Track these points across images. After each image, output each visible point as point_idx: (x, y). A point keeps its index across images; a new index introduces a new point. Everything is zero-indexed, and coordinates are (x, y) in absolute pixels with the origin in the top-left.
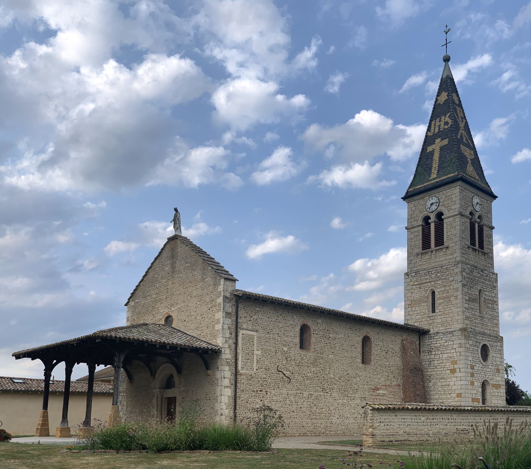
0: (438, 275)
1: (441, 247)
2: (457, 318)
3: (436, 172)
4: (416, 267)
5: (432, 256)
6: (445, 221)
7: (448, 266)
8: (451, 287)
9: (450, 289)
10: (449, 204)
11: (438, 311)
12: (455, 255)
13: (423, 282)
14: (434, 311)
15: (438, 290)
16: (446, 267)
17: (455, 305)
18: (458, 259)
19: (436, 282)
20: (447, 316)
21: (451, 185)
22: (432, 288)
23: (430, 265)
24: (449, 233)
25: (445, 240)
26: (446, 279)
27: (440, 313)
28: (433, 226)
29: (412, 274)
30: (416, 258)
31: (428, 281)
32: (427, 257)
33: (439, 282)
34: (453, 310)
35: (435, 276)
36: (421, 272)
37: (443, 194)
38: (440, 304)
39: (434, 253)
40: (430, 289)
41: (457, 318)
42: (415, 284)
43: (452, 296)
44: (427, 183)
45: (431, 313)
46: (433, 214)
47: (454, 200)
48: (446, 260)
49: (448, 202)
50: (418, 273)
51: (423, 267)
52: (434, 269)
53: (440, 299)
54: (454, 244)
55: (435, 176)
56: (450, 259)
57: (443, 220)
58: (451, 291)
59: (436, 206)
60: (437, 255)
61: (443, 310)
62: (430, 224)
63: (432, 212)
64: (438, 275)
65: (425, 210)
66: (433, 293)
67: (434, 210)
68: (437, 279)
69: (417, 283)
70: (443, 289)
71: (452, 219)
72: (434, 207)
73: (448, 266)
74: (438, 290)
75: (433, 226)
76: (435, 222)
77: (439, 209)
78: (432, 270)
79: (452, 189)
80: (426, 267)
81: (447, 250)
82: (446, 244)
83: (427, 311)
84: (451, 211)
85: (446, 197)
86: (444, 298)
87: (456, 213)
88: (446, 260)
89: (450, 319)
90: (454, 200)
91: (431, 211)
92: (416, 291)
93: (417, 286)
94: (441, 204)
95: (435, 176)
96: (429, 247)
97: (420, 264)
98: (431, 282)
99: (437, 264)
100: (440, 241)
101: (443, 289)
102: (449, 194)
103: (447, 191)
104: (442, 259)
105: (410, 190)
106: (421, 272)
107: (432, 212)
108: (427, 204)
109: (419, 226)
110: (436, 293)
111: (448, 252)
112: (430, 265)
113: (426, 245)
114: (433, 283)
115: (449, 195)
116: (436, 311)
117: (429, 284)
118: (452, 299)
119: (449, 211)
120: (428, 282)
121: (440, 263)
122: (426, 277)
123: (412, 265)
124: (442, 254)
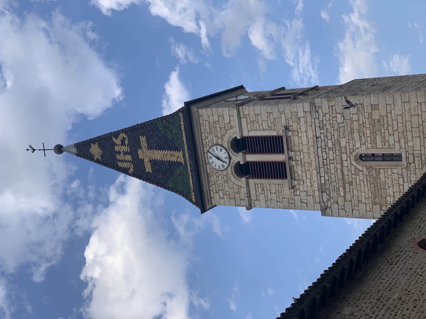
0: (330, 145)
1: (284, 140)
2: (413, 103)
3: (176, 153)
4: (314, 192)
5: (298, 158)
6: (245, 134)
7: (317, 125)
8: (355, 117)
9: (358, 120)
10: (222, 126)
11: (397, 145)
12: (301, 114)
13: (340, 176)
14: (397, 158)
15: (358, 145)
16: (317, 129)
17: (389, 109)
18: (307, 107)
19: (343, 150)
20: (409, 127)
21: (195, 122)
22: (352, 158)
23: (313, 163)
24: (265, 127)
25: (274, 134)
26: (338, 130)
27: (402, 141)
28: (252, 158)
29: (325, 200)
30: (298, 192)
31: (339, 166)
32: (298, 170)
33: (343, 144)
34: (397, 113)
35: (331, 153)
36: (323, 182)
37: (207, 137)
38: (384, 141)
39: (292, 154)
40: (354, 163)
41: (413, 103)
42: (342, 194)
43: (370, 115)
44: (189, 166)
45: (400, 163)
46: (233, 157)
47: (216, 118)
48: (306, 132)
49: (218, 130)
50: (324, 187)
51: (315, 178)
52: (320, 154)
53: (374, 141)
54: (283, 115)
55: (181, 154)
56: (306, 122)
57: (244, 139)
58: (361, 118)
59: (221, 150)
60: (297, 148)
61: (396, 133)
62: (247, 164)
63: (230, 158)
64: (330, 145)
65: (225, 172)
66: (362, 158)
67: (226, 155)
68: (337, 147)
69: (341, 189)
70: (356, 135)
71: (244, 121)
72: (223, 155)
73: (317, 125)
74: (358, 145)
75: (252, 158)
76: (245, 154)
77: (226, 147)
78: (321, 158)
79: (201, 122)
80: (315, 172)
81: (291, 128)
82: (281, 133)
83: (395, 171)
84: (232, 124)
85: (211, 132)
86: (373, 133)
87: (235, 111)
88: (306, 132)
89: (415, 120)
90: (216, 118)
91: (227, 160)
92: (355, 191)
93: (347, 190)
94: (220, 142)
95: (181, 154)
96: (282, 165)
97: (309, 184)
98: (342, 161)
99: (312, 149)
100: (274, 144)
101: (356, 135)
102: (208, 128)
103: (203, 131)
104: (304, 139)
105: (194, 200)
106: (323, 182)
107: (230, 158)
108: (217, 167)
109: (248, 184)
110: (363, 150)
111: (295, 126)
112: (313, 163)
113: (278, 171)
114: (344, 156)
115: (210, 126)
116: (396, 151)
117: (345, 163)
118: (376, 115)
119: (232, 127)
120: (342, 166)
121: (311, 144)
122: (333, 171)
123: (310, 200)
124: (296, 139)
